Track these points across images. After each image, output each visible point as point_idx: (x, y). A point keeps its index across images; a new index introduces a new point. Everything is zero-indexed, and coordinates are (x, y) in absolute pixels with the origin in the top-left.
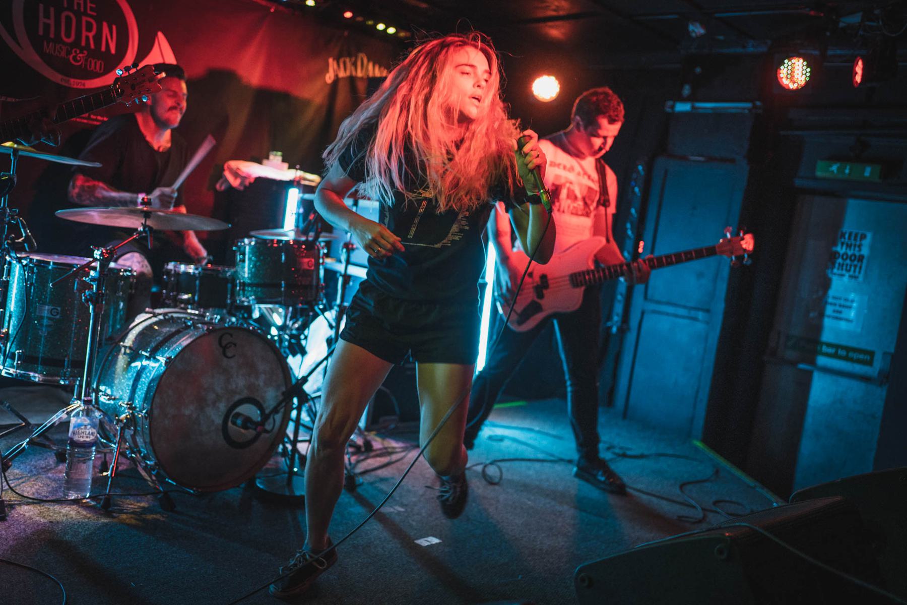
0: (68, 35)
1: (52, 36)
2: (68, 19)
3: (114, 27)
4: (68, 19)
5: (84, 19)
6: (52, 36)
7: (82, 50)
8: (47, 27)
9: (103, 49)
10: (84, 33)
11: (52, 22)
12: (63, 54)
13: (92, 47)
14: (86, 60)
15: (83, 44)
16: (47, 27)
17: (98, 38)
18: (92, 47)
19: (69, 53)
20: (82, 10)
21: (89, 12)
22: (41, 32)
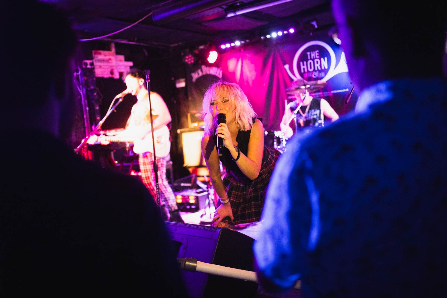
0: (311, 68)
1: (306, 70)
2: (310, 63)
3: (326, 58)
4: (310, 63)
5: (316, 60)
6: (306, 70)
7: (316, 71)
8: (304, 69)
9: (323, 68)
10: (316, 65)
11: (305, 67)
12: (311, 75)
13: (319, 68)
14: (318, 74)
15: (316, 69)
16: (304, 69)
17: (321, 66)
18: (319, 68)
19: (312, 74)
20: (314, 57)
21: (317, 57)
22: (302, 71)
